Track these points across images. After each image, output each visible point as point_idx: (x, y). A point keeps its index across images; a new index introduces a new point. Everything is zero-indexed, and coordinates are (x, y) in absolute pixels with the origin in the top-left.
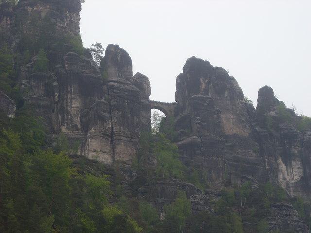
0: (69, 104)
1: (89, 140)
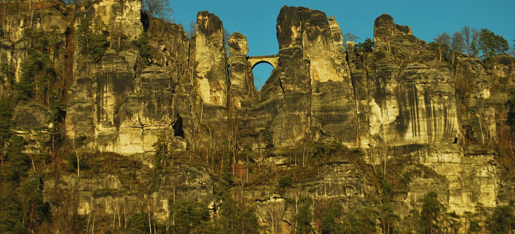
0: (105, 103)
1: (120, 135)
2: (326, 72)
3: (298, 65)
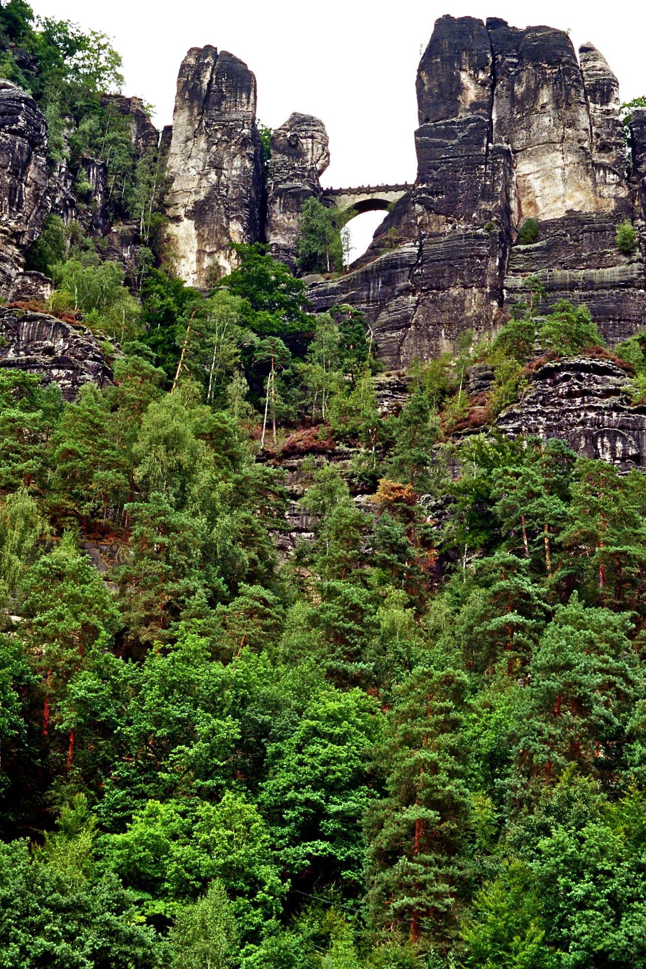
2: (561, 189)
3: (472, 165)
